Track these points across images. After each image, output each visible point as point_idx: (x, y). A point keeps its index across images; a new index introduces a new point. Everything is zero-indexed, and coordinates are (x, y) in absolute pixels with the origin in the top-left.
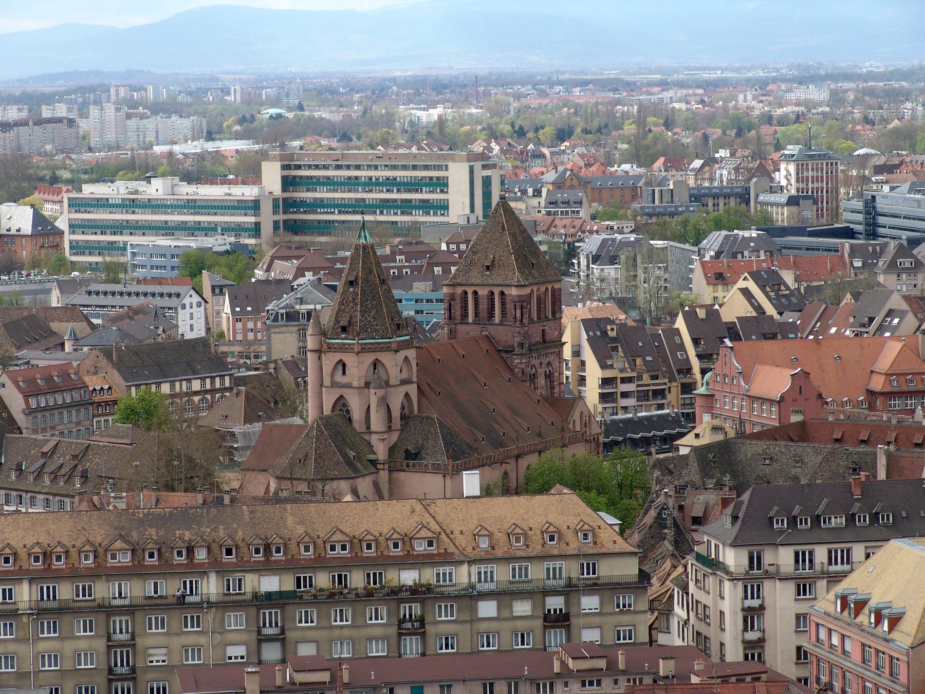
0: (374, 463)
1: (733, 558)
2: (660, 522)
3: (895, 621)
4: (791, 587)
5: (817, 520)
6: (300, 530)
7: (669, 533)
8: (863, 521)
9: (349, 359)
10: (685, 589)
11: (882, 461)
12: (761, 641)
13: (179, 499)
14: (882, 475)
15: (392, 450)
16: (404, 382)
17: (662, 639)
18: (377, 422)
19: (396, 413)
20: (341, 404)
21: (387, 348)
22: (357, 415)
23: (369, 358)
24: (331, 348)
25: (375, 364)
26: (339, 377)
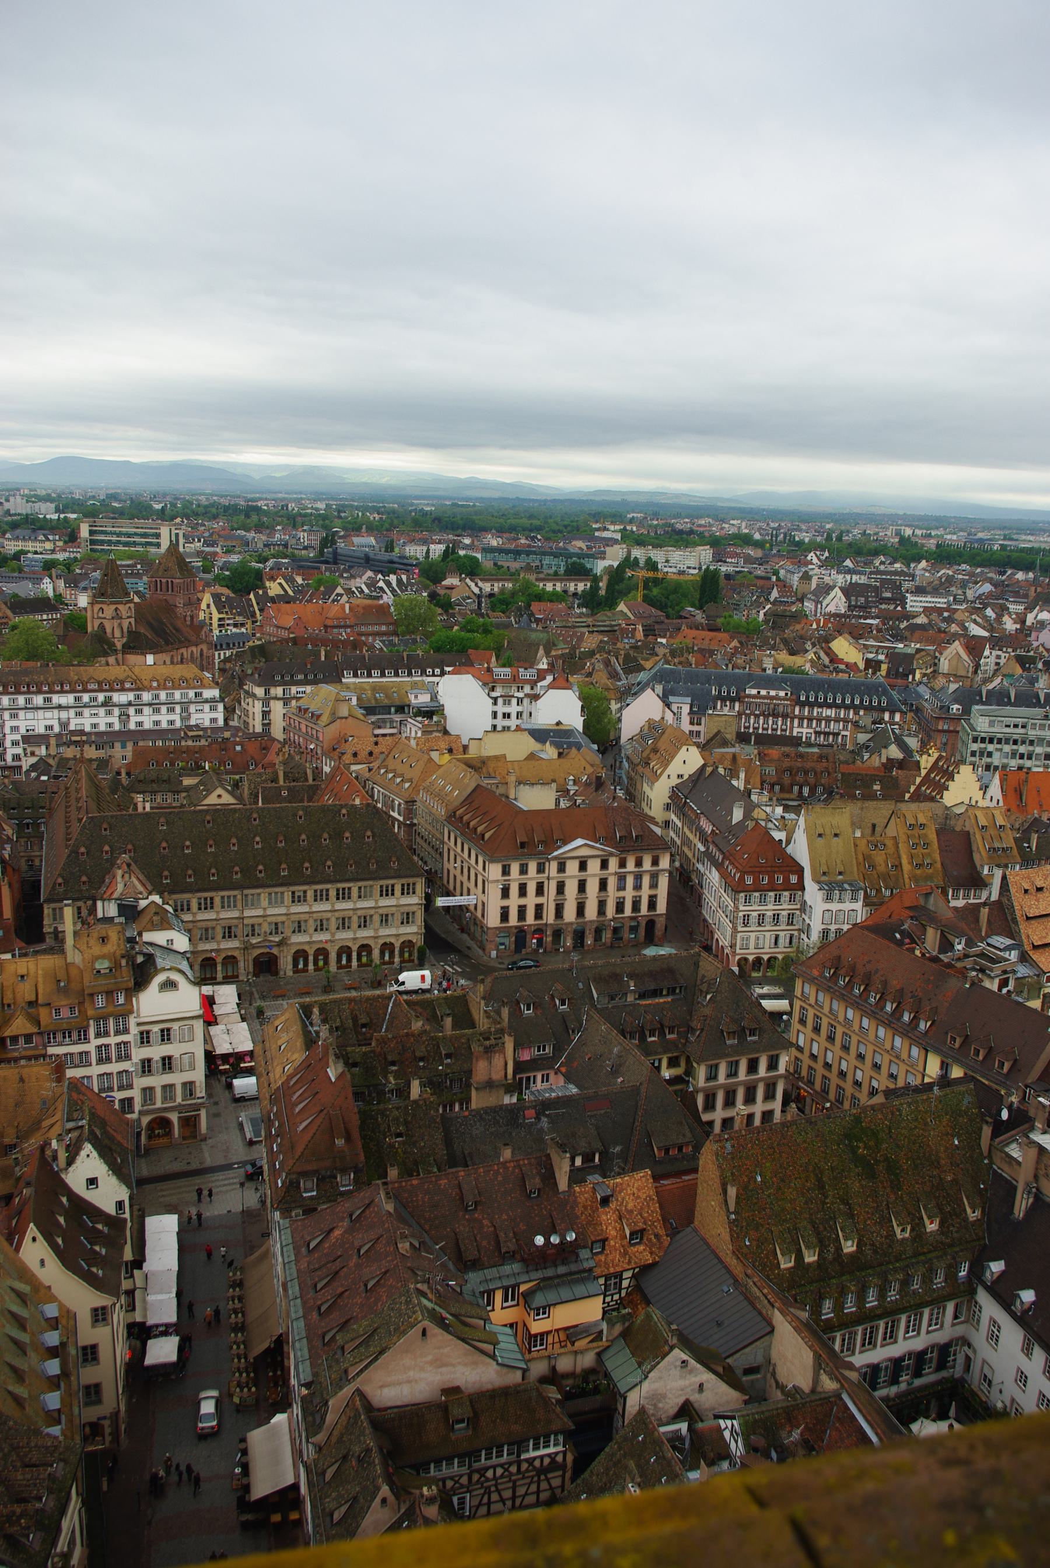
0: (116, 650)
1: (259, 691)
2: (233, 677)
3: (319, 717)
4: (280, 704)
5: (292, 676)
6: (76, 678)
7: (237, 681)
8: (311, 677)
9: (104, 607)
10: (240, 704)
11: (323, 653)
12: (269, 724)
13: (31, 664)
14: (323, 659)
15: (124, 646)
16: (129, 617)
17: (231, 723)
18: (117, 634)
19: (125, 630)
20: (102, 626)
21: (121, 603)
22: (109, 630)
23: (113, 607)
24: (97, 602)
25: (116, 609)
26: (100, 615)
